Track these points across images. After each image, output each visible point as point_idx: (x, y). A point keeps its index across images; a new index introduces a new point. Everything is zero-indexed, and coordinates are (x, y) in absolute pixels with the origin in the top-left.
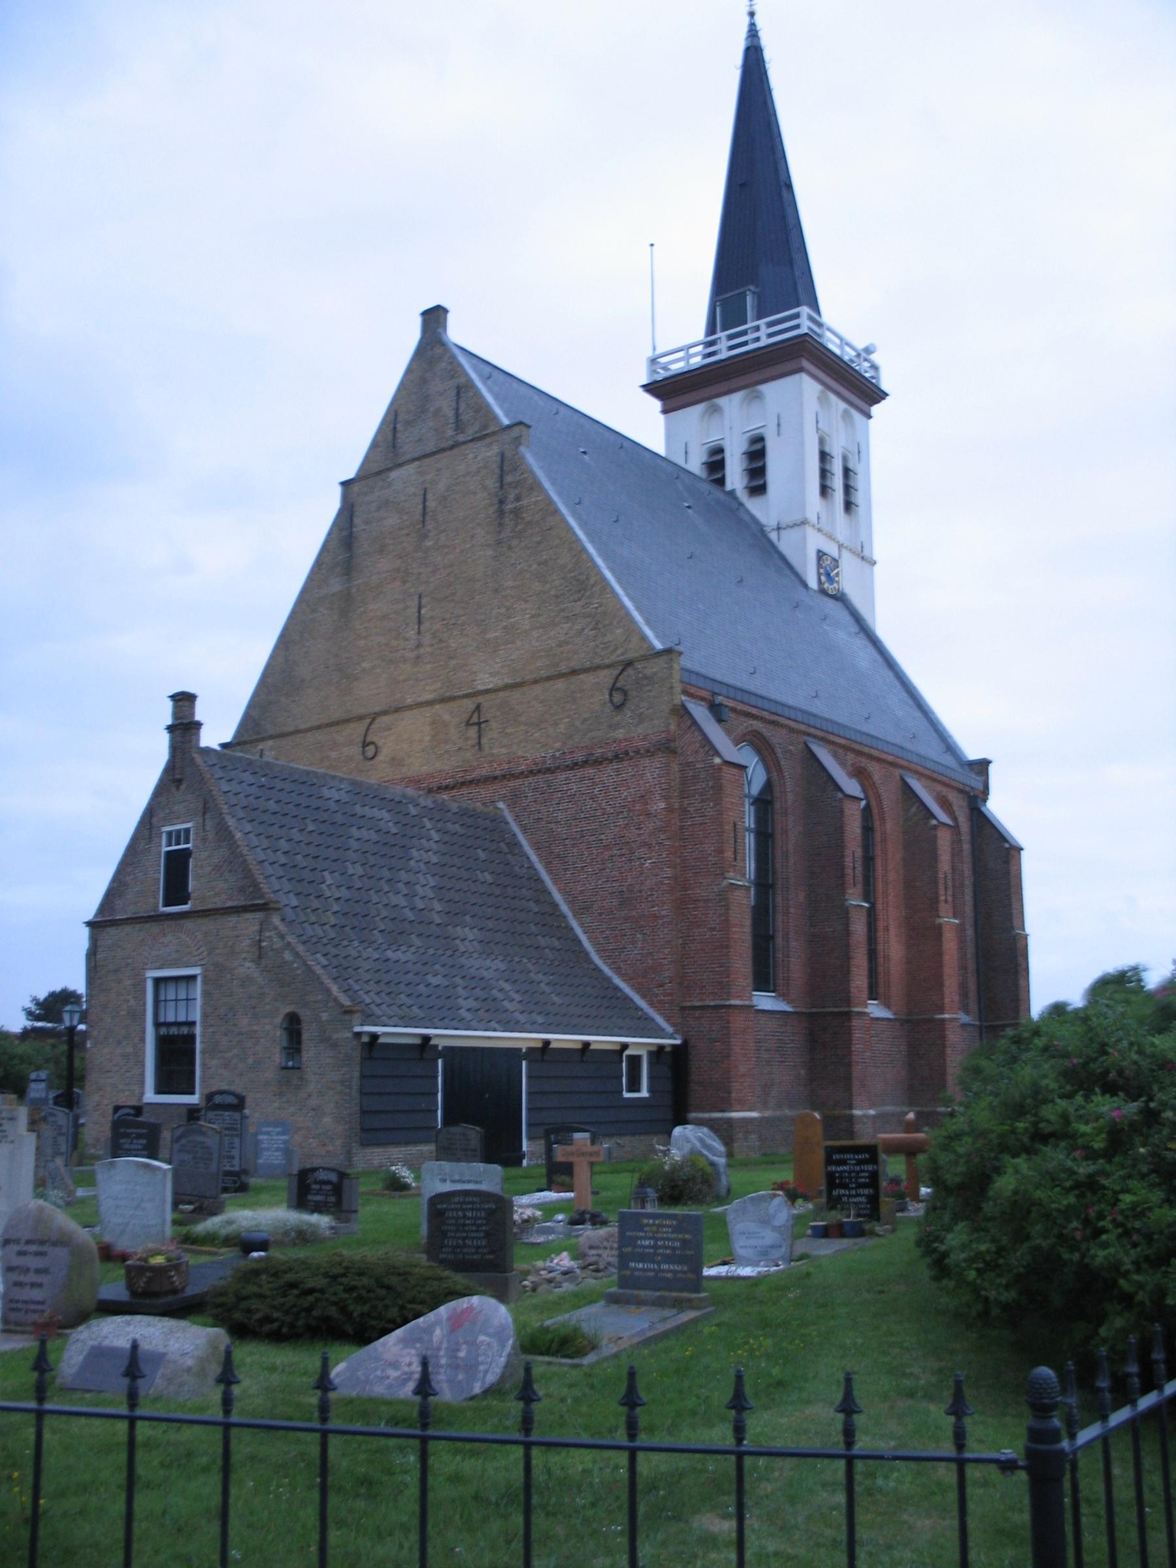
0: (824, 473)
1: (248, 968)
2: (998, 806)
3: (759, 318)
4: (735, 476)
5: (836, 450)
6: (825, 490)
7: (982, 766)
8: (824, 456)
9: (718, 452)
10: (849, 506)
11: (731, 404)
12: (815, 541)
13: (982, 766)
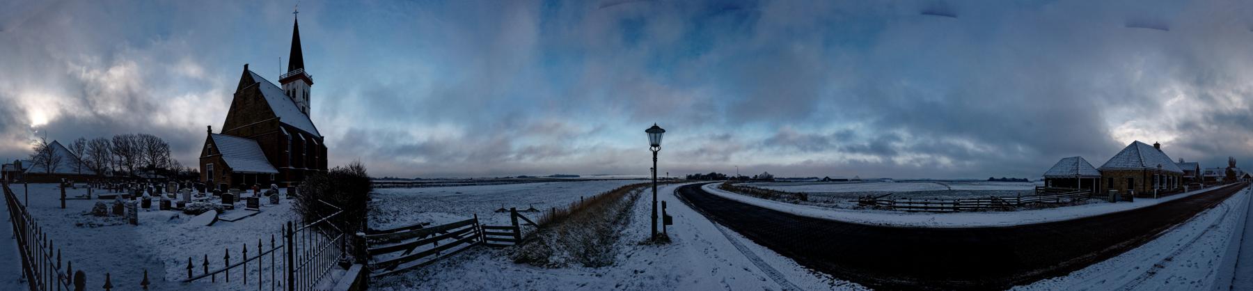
0: (304, 95)
1: (218, 163)
2: (324, 142)
3: (296, 69)
4: (291, 95)
5: (306, 91)
6: (304, 97)
7: (323, 137)
8: (304, 92)
9: (289, 91)
10: (307, 100)
11: (291, 84)
12: (302, 105)
13: (323, 137)
